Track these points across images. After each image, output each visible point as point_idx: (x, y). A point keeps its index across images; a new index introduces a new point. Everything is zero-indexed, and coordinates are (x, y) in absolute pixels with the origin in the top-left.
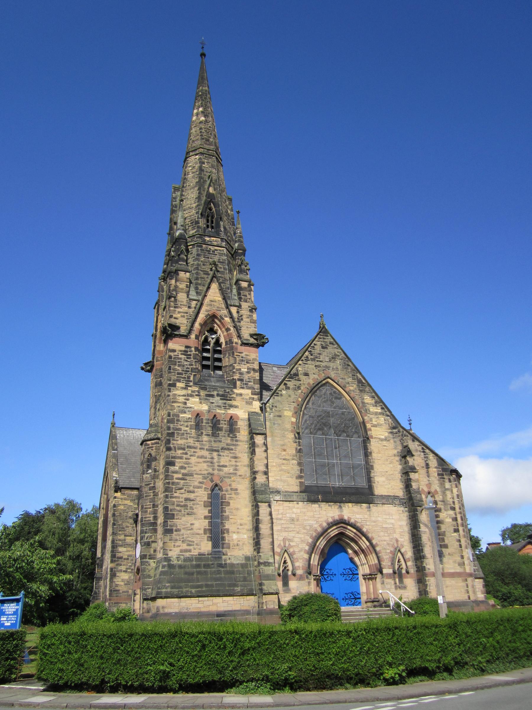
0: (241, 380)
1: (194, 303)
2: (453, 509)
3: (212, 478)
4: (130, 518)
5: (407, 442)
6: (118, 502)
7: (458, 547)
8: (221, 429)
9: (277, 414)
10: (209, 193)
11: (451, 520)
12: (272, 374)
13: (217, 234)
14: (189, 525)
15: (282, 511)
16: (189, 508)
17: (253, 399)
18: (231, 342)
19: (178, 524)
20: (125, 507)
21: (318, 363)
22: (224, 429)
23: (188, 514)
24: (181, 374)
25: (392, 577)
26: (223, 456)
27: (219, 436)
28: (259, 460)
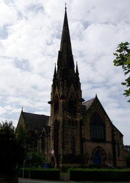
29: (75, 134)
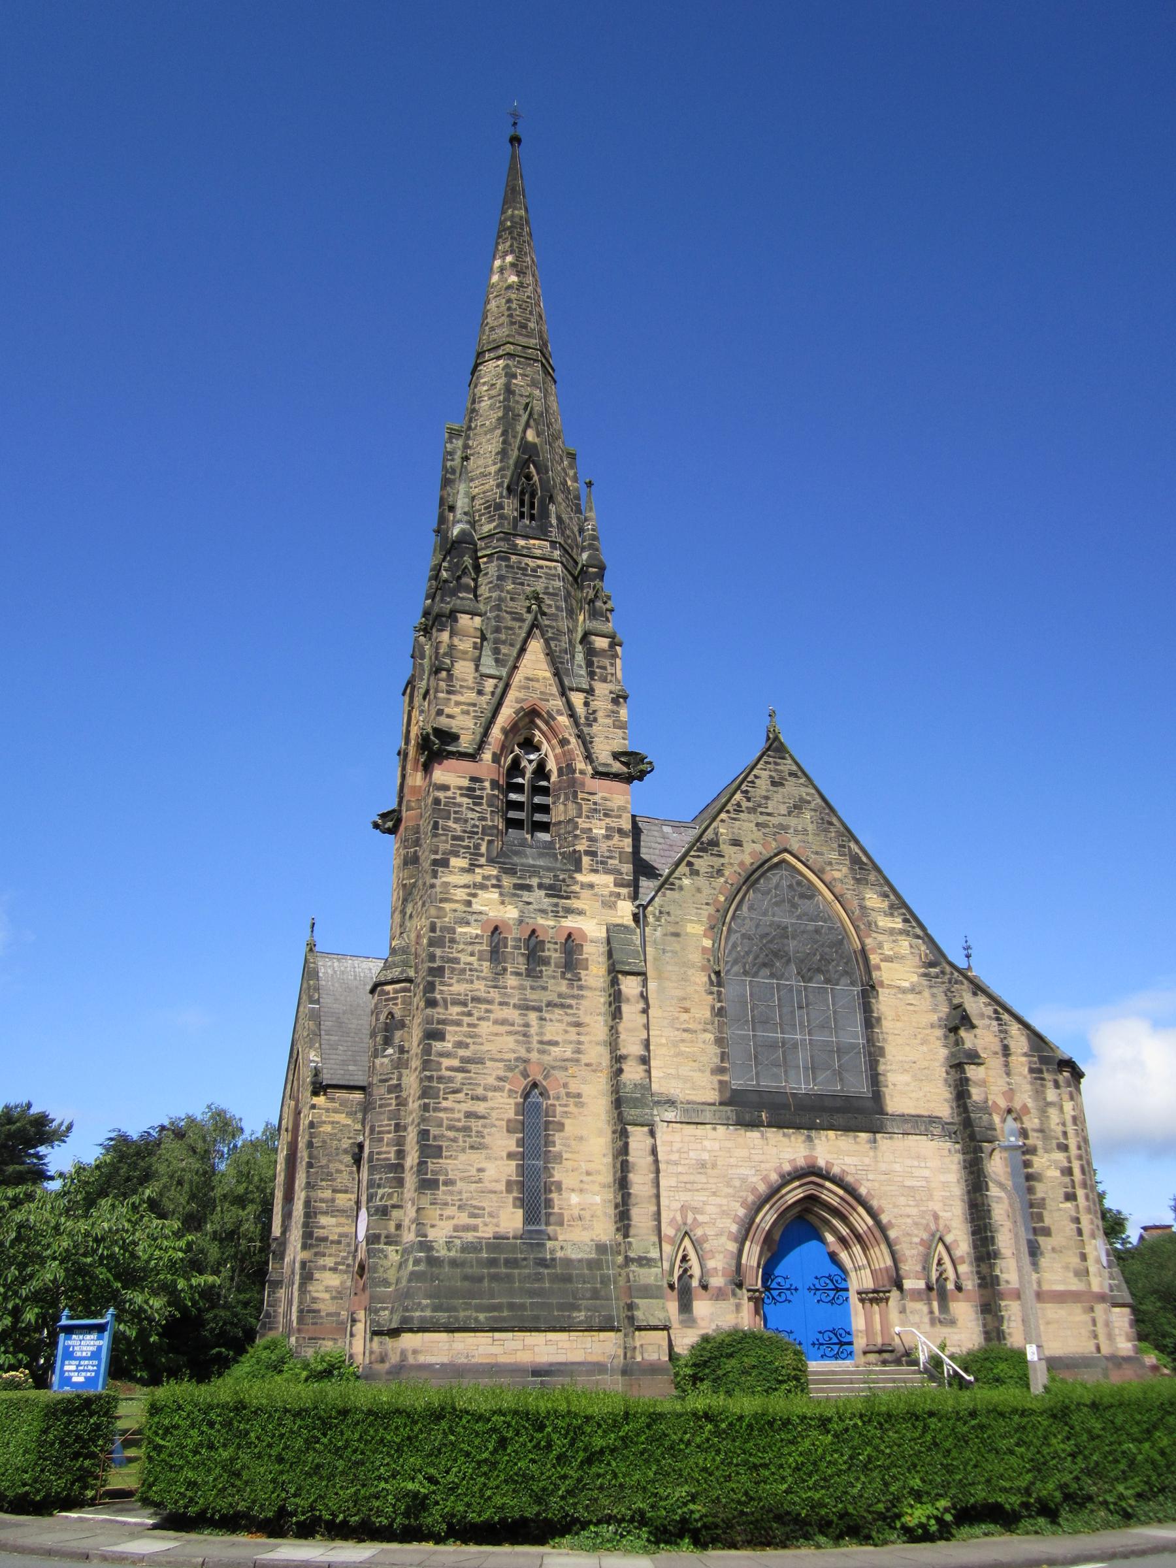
0: (592, 854)
1: (489, 684)
2: (1064, 1148)
3: (525, 1069)
4: (346, 1151)
5: (961, 997)
6: (320, 1117)
7: (1075, 1233)
8: (546, 962)
9: (671, 929)
10: (527, 442)
11: (1057, 1173)
12: (661, 840)
13: (542, 533)
14: (473, 1172)
15: (680, 1145)
16: (473, 1134)
17: (618, 895)
18: (570, 769)
19: (449, 1168)
20: (334, 1128)
21: (762, 819)
22: (552, 961)
23: (472, 1147)
24: (461, 839)
25: (924, 1297)
26: (551, 1020)
27: (541, 977)
28: (628, 1030)
29: (555, 1050)
